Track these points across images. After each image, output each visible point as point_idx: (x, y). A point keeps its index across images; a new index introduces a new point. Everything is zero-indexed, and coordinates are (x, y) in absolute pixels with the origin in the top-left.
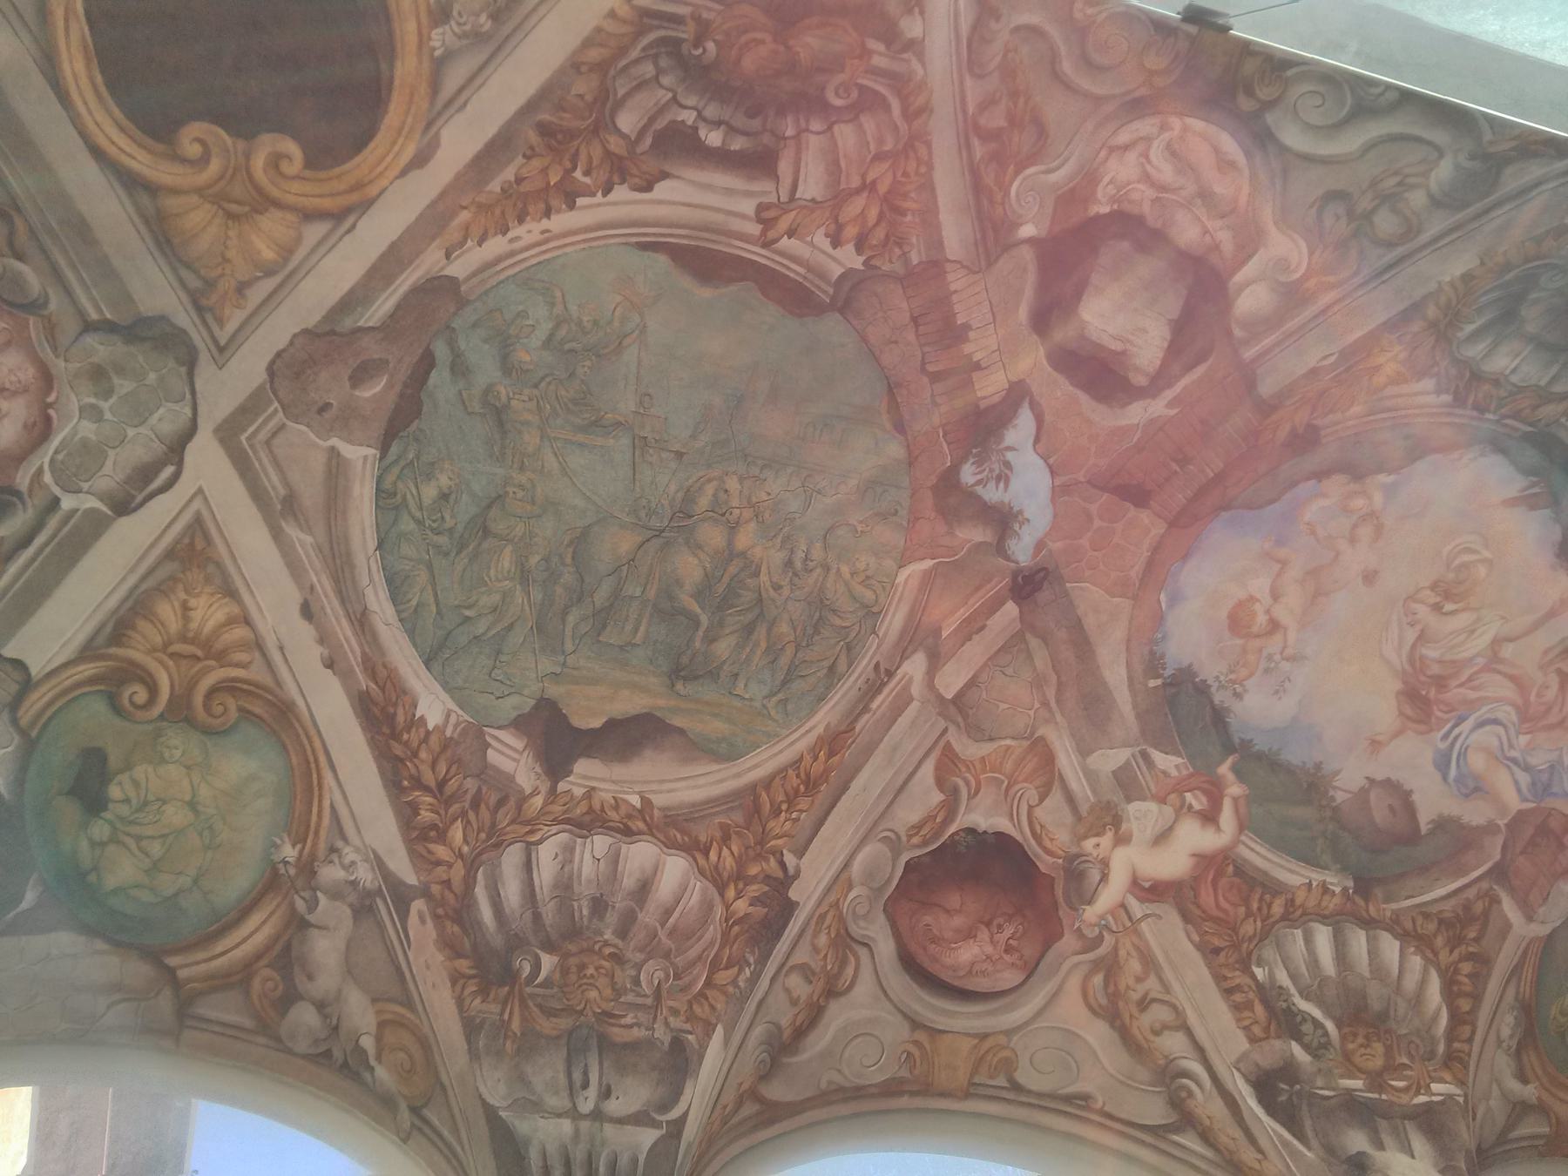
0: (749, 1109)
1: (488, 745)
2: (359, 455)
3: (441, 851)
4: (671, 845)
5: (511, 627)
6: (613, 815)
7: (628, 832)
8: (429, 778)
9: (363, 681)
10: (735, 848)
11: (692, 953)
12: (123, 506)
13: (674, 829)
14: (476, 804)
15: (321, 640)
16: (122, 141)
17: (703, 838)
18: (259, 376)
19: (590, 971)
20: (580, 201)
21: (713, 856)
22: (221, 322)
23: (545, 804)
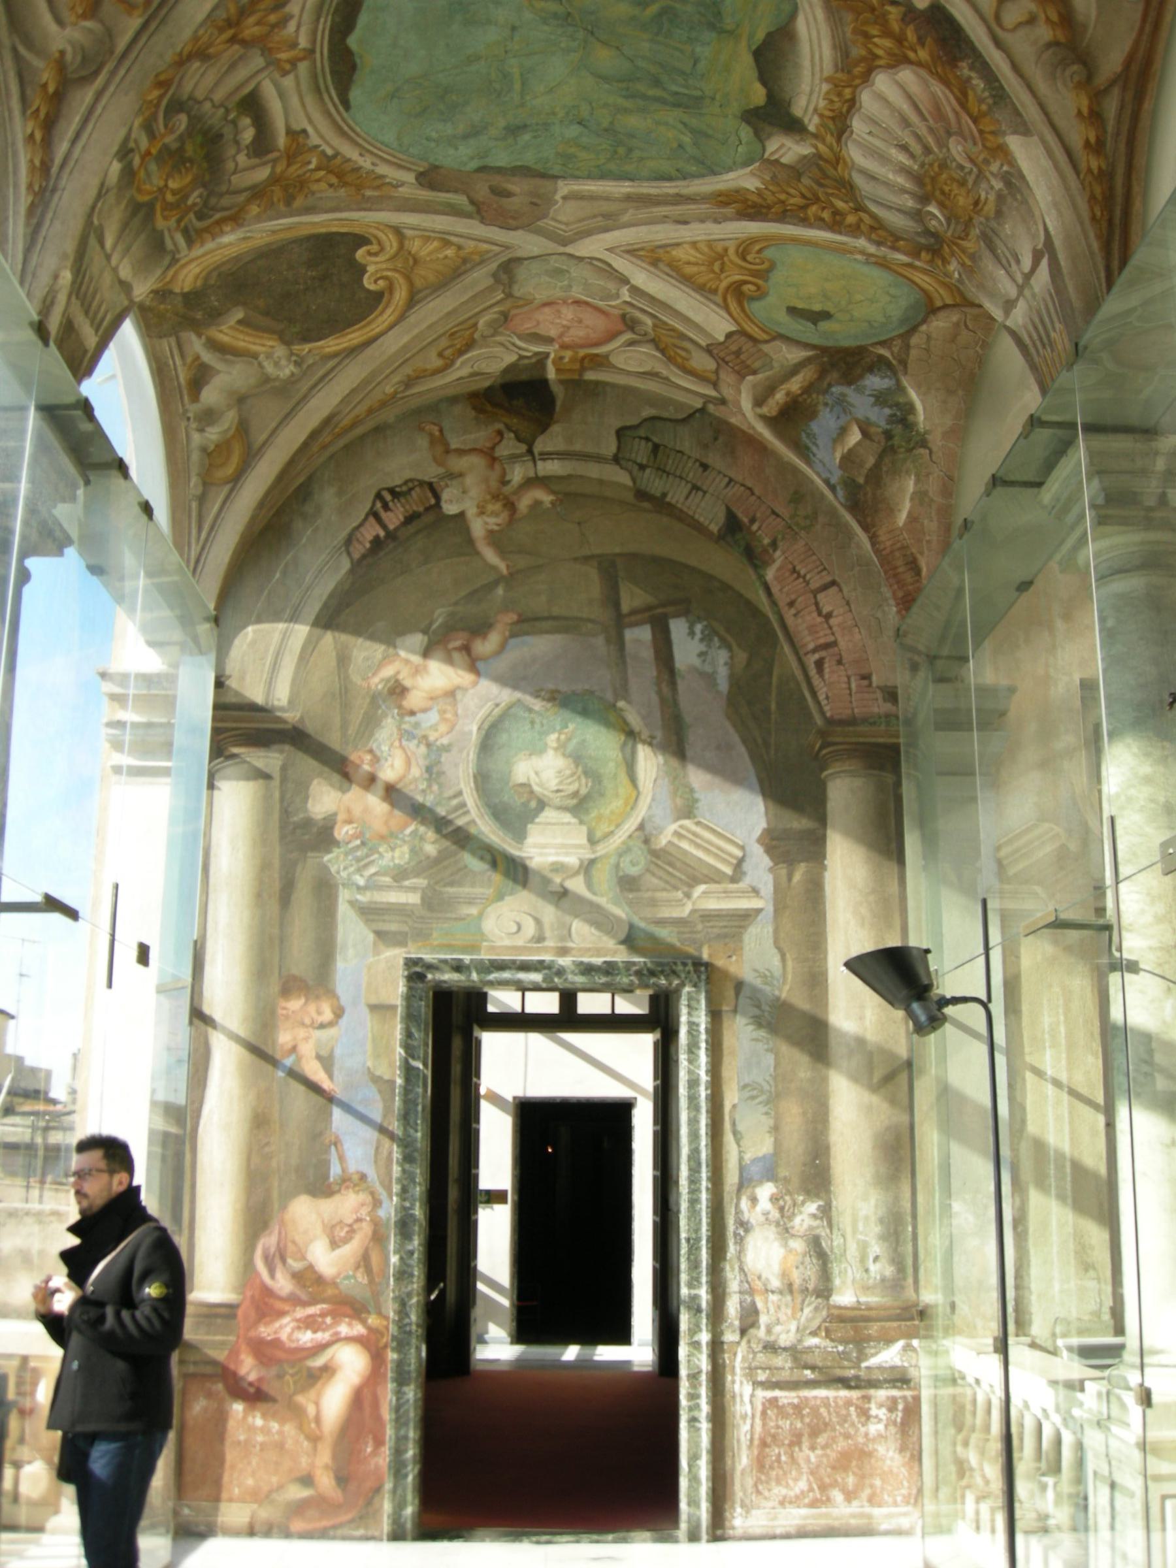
0: (1111, 107)
1: (777, 161)
2: (564, 188)
3: (851, 219)
4: (866, 77)
5: (685, 124)
6: (837, 105)
7: (852, 103)
8: (798, 201)
9: (729, 211)
10: (875, 32)
11: (951, 115)
12: (625, 281)
13: (853, 72)
14: (821, 185)
15: (702, 221)
16: (389, 311)
17: (863, 53)
18: (520, 233)
19: (947, 189)
20: (330, 152)
21: (880, 52)
22: (488, 252)
23: (824, 141)
